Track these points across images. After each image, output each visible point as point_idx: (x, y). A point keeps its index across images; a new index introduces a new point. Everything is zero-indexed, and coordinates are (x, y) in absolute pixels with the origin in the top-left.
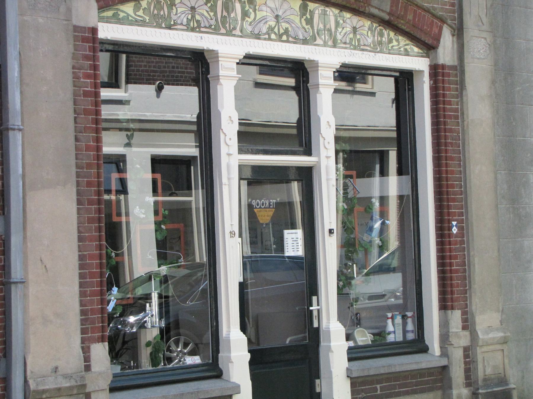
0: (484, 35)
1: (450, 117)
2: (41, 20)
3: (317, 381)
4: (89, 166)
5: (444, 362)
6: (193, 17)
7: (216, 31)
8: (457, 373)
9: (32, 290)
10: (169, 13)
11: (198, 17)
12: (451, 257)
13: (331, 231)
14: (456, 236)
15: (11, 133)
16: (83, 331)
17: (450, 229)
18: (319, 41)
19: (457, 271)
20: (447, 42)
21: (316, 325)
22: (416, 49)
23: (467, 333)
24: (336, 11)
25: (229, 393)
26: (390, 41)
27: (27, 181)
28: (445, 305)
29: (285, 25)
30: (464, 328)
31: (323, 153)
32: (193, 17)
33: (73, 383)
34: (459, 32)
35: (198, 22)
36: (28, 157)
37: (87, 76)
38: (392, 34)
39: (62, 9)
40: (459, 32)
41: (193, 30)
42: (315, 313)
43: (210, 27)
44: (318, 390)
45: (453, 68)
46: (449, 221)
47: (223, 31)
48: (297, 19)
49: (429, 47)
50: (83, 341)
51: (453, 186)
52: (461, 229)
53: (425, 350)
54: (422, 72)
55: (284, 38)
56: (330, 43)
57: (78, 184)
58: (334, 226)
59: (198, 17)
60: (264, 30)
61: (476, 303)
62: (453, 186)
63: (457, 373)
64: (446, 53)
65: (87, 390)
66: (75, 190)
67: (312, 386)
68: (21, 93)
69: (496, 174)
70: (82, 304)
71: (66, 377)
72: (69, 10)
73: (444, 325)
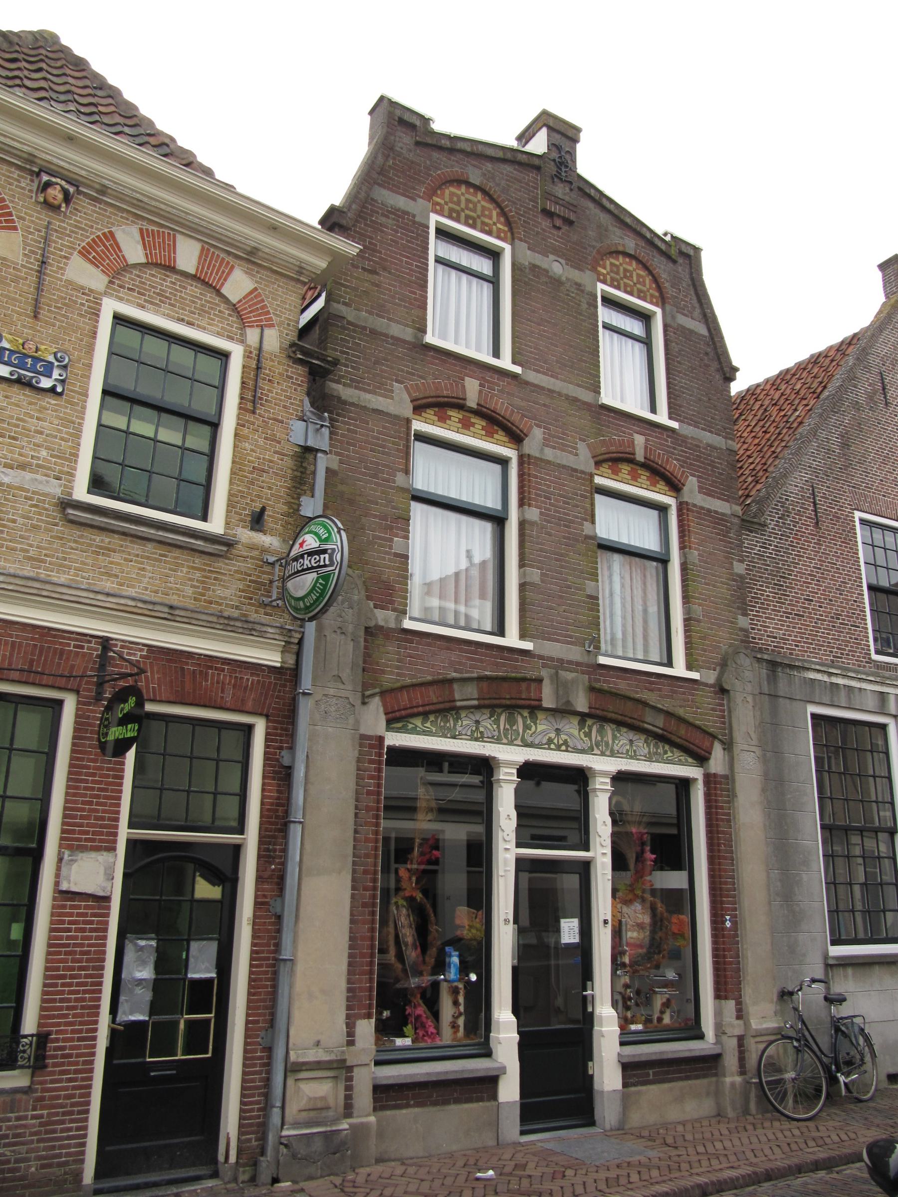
0: (753, 748)
1: (722, 820)
2: (330, 729)
3: (590, 1064)
4: (367, 856)
5: (717, 1050)
6: (477, 728)
7: (498, 741)
8: (731, 1061)
9: (300, 968)
10: (455, 725)
11: (481, 729)
12: (724, 950)
13: (606, 922)
14: (730, 929)
15: (292, 826)
16: (349, 1008)
17: (724, 922)
18: (596, 751)
19: (731, 963)
20: (718, 755)
21: (590, 1010)
22: (690, 760)
23: (740, 1022)
24: (614, 726)
25: (495, 1073)
26: (666, 752)
27: (304, 868)
28: (720, 993)
29: (564, 737)
30: (739, 1017)
31: (600, 850)
32: (477, 728)
33: (332, 1057)
34: (728, 746)
35: (481, 733)
36: (308, 846)
37: (371, 777)
38: (667, 747)
39: (351, 720)
40: (728, 746)
41: (476, 740)
42: (590, 999)
43: (493, 737)
44: (590, 1072)
45: (726, 777)
46: (723, 916)
47: (505, 741)
48: (576, 732)
49: (701, 759)
50: (348, 1017)
51: (726, 883)
52: (735, 923)
53: (701, 1036)
54: (695, 780)
55: (563, 748)
56: (608, 753)
57: (354, 871)
58: (609, 917)
59: (481, 729)
60: (545, 741)
61: (748, 993)
62: (726, 883)
63: (731, 1061)
64: (717, 762)
65: (348, 1063)
66: (350, 877)
67: (586, 1068)
68: (305, 791)
69: (768, 873)
70: (349, 981)
71: (327, 1050)
72: (357, 722)
73: (718, 1013)
